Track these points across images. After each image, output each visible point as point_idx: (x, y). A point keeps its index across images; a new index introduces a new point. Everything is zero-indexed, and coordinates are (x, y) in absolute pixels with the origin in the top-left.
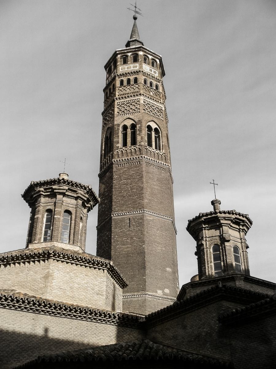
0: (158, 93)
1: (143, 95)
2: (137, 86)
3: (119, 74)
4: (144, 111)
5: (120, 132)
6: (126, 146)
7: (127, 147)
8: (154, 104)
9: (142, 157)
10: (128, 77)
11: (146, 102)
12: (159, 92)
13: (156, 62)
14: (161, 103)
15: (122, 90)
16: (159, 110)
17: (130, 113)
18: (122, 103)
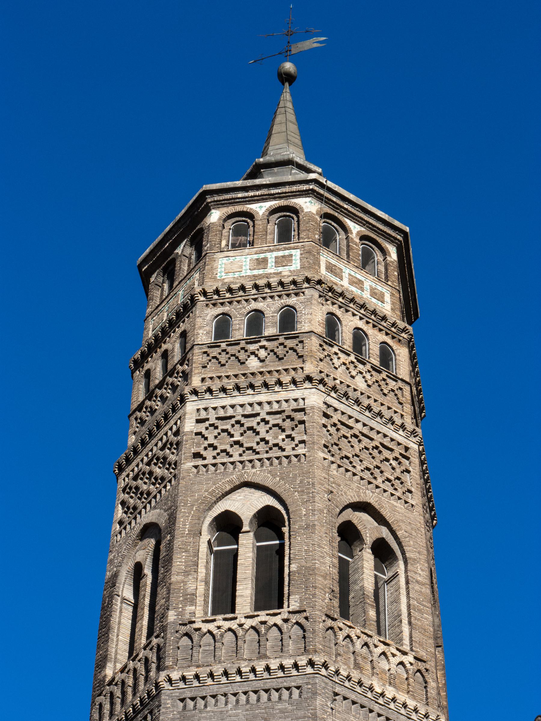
0: (392, 384)
2: (290, 343)
3: (210, 290)
4: (322, 455)
5: (204, 548)
6: (233, 611)
7: (235, 618)
8: (372, 429)
9: (311, 663)
10: (254, 305)
11: (335, 419)
12: (396, 379)
13: (384, 252)
14: (403, 426)
15: (223, 358)
16: (396, 459)
17: (260, 460)
18: (221, 413)
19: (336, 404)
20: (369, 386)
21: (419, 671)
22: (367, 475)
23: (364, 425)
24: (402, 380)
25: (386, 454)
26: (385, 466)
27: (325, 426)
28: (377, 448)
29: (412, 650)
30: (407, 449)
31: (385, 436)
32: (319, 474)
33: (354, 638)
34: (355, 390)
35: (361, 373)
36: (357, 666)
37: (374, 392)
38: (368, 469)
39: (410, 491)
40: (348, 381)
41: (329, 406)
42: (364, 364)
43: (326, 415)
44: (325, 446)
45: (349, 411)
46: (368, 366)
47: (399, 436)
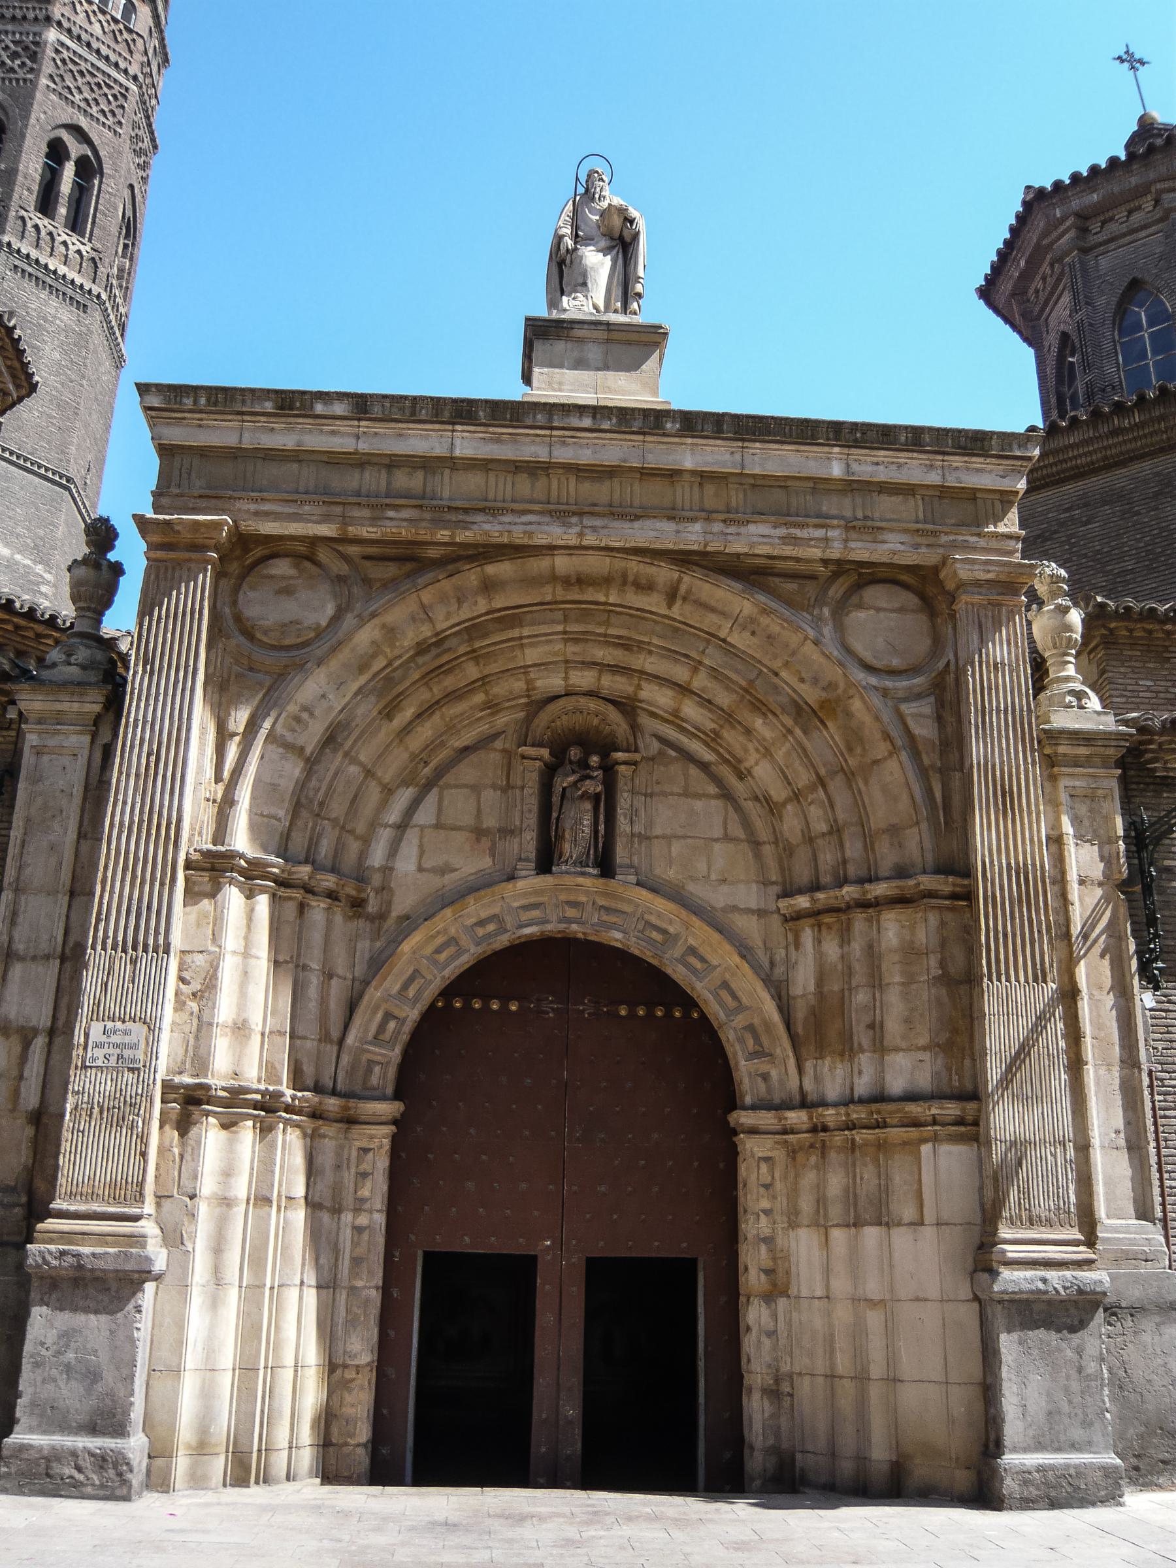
0: (126, 35)
1: (59, 24)
14: (126, 71)
19: (68, 42)
20: (104, 32)
21: (93, 259)
22: (83, 105)
23: (92, 64)
24: (137, 34)
25: (105, 90)
26: (102, 100)
27: (54, 60)
28: (98, 85)
29: (90, 240)
30: (127, 89)
31: (109, 76)
32: (39, 95)
33: (41, 227)
34: (92, 35)
35: (100, 21)
36: (37, 246)
37: (109, 40)
38: (86, 100)
39: (120, 123)
40: (86, 25)
41: (62, 44)
42: (104, 12)
43: (57, 51)
44: (51, 76)
45: (79, 50)
46: (108, 17)
47: (121, 78)
